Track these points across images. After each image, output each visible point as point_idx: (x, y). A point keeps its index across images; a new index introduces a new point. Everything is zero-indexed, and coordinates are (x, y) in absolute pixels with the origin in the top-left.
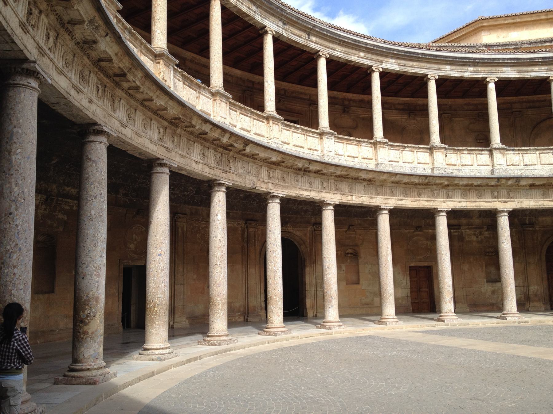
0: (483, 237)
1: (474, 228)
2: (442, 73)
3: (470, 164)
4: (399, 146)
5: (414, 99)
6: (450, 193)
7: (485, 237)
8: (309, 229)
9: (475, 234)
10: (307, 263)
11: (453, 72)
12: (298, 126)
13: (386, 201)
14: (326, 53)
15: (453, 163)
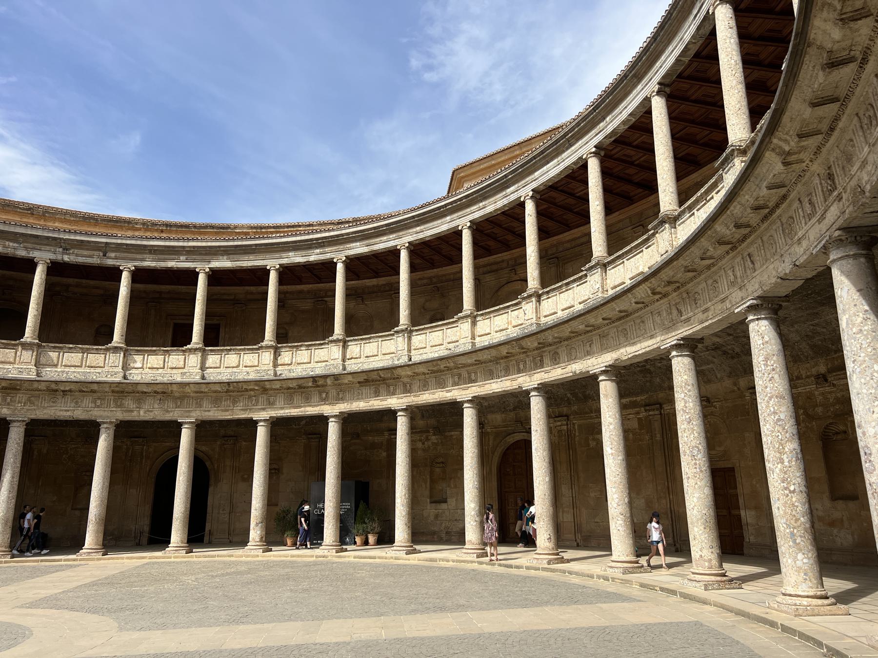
0: (430, 443)
1: (419, 432)
2: (285, 261)
3: (305, 361)
4: (222, 350)
5: (360, 282)
6: (272, 399)
7: (433, 443)
8: (218, 443)
9: (420, 440)
10: (212, 481)
11: (296, 258)
12: (71, 346)
13: (187, 414)
14: (129, 266)
15: (286, 362)
